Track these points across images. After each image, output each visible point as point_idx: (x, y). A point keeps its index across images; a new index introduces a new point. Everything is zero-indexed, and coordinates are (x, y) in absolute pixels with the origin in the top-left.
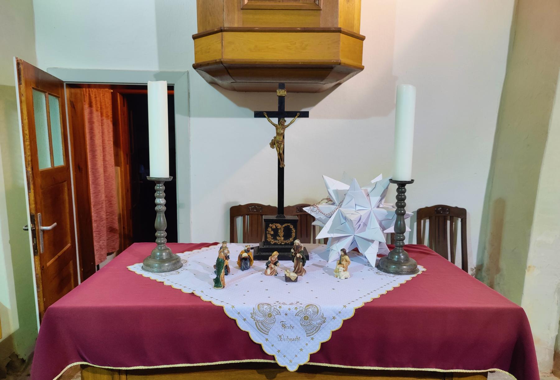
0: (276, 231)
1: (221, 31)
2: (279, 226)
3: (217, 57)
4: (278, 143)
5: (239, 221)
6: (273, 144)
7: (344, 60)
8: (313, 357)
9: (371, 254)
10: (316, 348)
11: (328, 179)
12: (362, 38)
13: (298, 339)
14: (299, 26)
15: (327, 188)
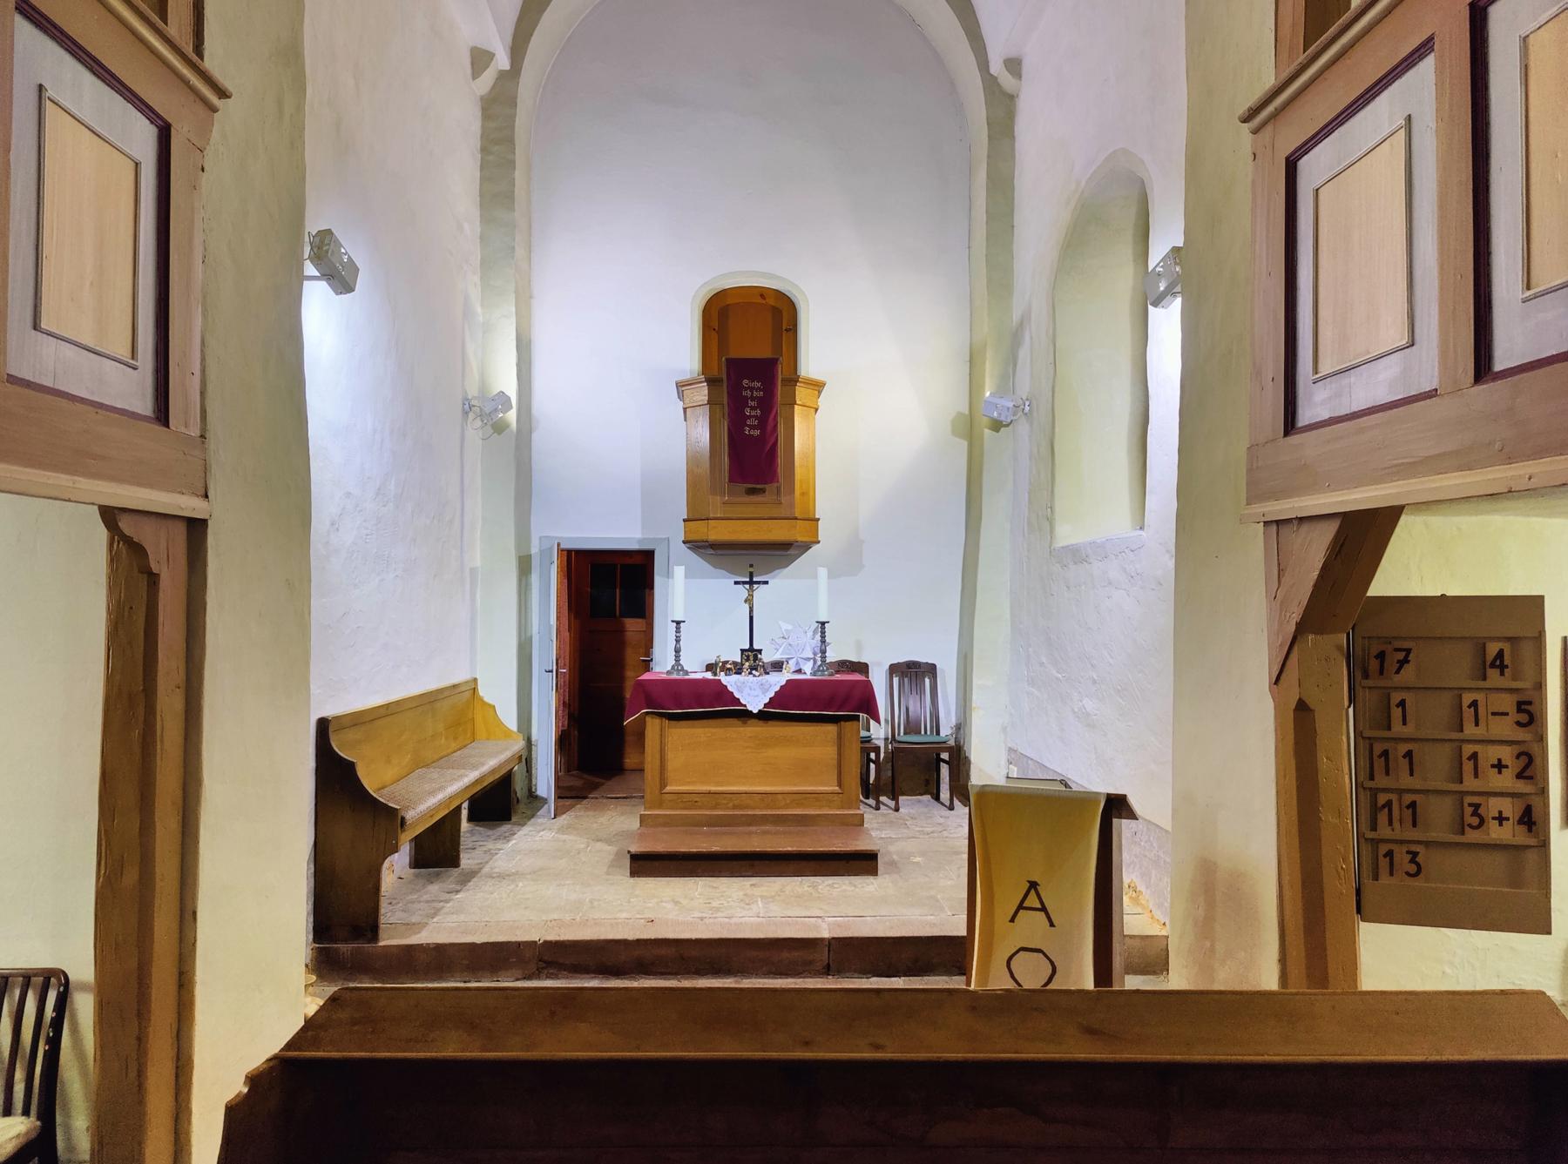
4: (749, 600)
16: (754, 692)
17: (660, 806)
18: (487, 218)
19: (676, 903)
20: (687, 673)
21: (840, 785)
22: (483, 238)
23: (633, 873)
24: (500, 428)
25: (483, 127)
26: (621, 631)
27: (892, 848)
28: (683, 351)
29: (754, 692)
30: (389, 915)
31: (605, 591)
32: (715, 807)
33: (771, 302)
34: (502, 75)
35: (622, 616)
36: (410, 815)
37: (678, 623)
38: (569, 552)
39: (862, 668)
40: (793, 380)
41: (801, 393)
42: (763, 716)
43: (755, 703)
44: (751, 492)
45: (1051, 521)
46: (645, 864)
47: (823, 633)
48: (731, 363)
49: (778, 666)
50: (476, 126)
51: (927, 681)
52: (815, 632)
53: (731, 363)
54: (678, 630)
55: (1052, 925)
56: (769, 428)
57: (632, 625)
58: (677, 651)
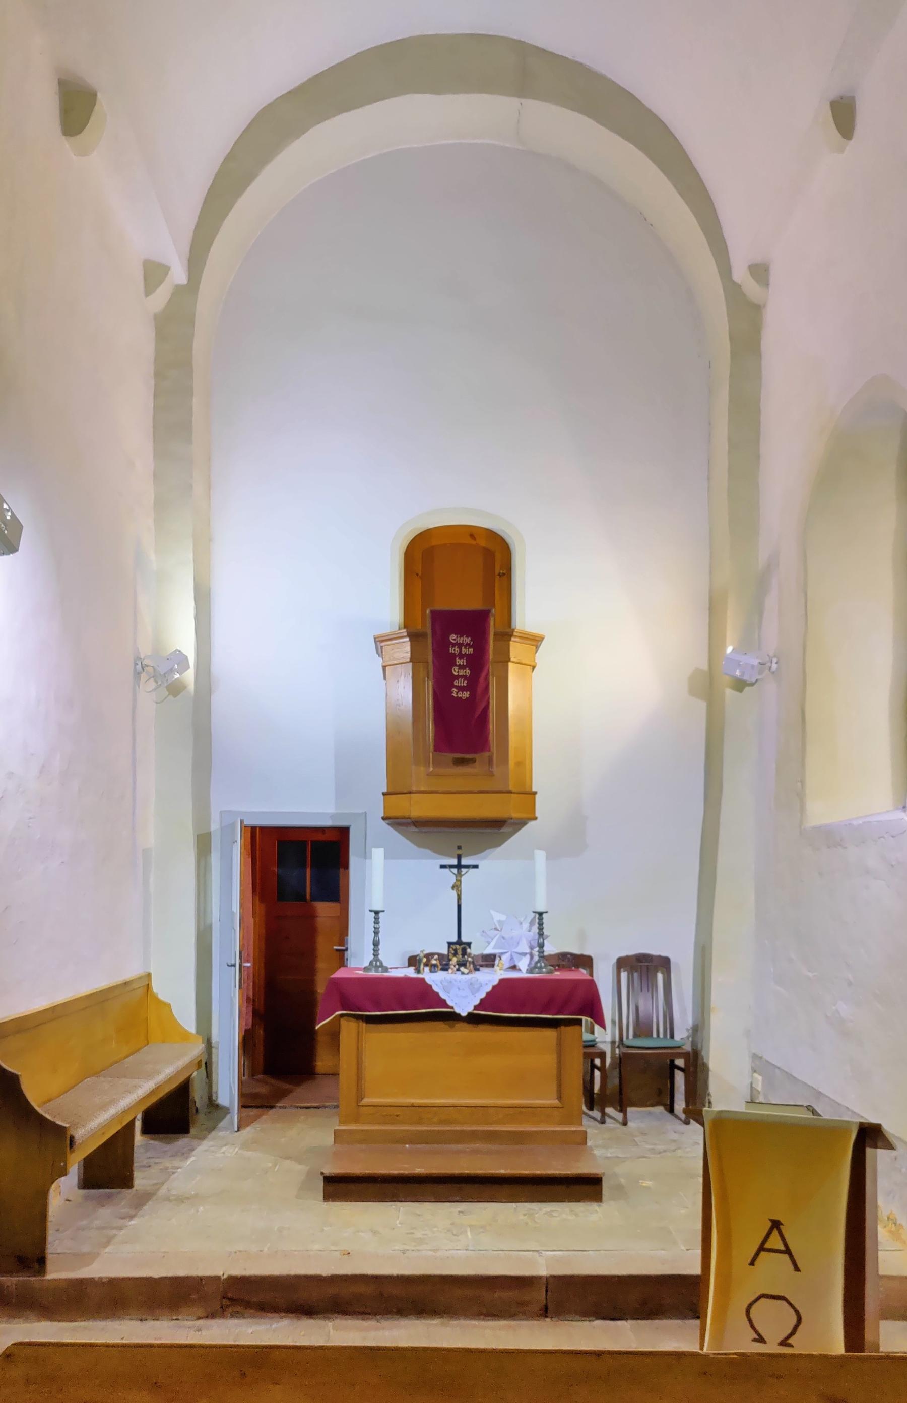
0: (456, 950)
1: (410, 793)
2: (458, 947)
3: (407, 814)
4: (457, 887)
6: (453, 888)
7: (515, 815)
8: (476, 1008)
10: (477, 1002)
11: (493, 912)
12: (535, 793)
13: (466, 997)
14: (476, 790)
15: (493, 919)
16: (462, 992)
17: (356, 1121)
18: (161, 452)
19: (375, 1233)
20: (386, 969)
21: (560, 1098)
24: (176, 689)
26: (311, 916)
29: (462, 992)
30: (57, 1244)
31: (297, 873)
32: (420, 1122)
34: (178, 290)
35: (314, 898)
36: (79, 1134)
37: (377, 913)
38: (253, 829)
39: (586, 962)
40: (507, 634)
41: (516, 649)
42: (473, 1019)
43: (464, 1005)
44: (459, 762)
45: (801, 796)
46: (340, 1187)
47: (541, 924)
48: (436, 616)
49: (489, 961)
50: (149, 350)
52: (532, 923)
53: (436, 616)
54: (377, 921)
55: (797, 1269)
56: (480, 690)
57: (324, 910)
58: (376, 944)
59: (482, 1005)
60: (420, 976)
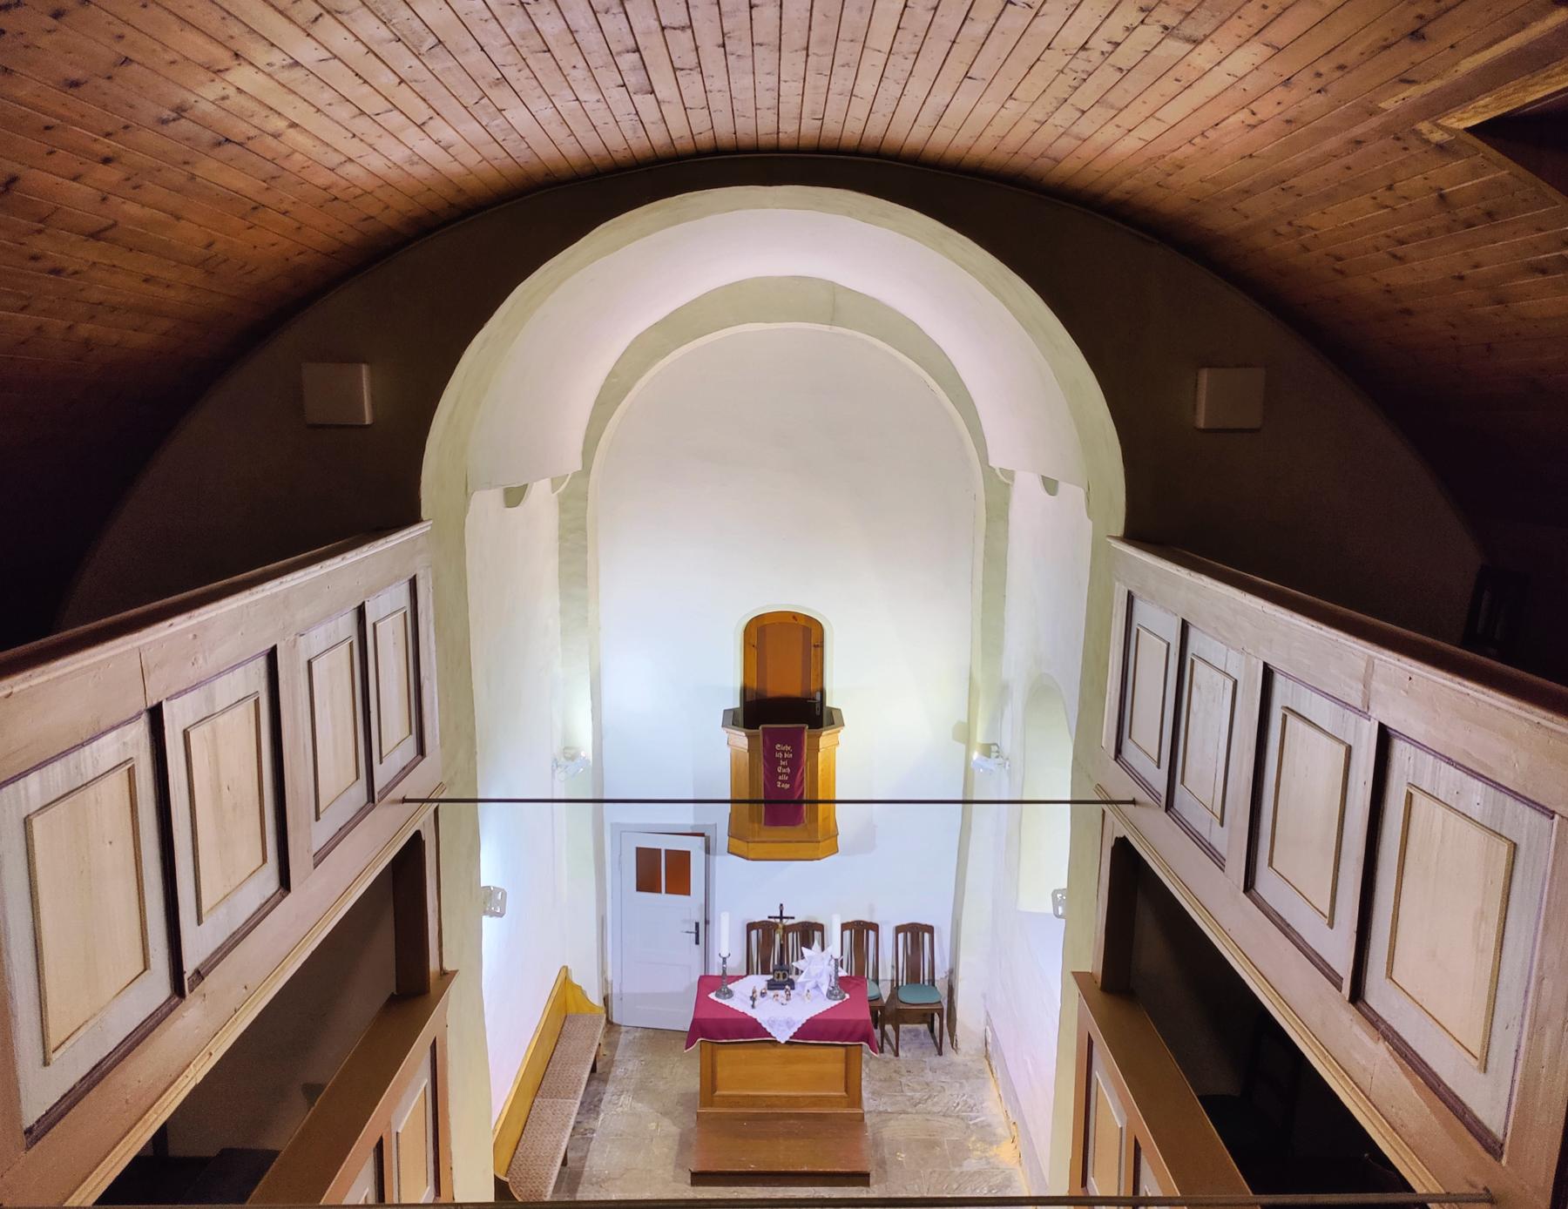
5: (754, 933)
9: (825, 989)
22: (562, 612)
23: (693, 1184)
25: (560, 520)
27: (886, 1134)
28: (726, 680)
32: (753, 1106)
33: (802, 622)
43: (783, 1036)
51: (927, 936)
59: (795, 1035)
60: (751, 1013)
